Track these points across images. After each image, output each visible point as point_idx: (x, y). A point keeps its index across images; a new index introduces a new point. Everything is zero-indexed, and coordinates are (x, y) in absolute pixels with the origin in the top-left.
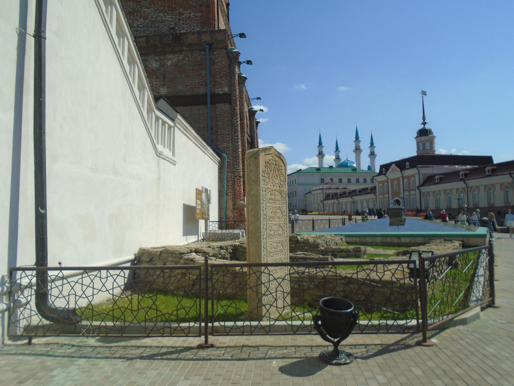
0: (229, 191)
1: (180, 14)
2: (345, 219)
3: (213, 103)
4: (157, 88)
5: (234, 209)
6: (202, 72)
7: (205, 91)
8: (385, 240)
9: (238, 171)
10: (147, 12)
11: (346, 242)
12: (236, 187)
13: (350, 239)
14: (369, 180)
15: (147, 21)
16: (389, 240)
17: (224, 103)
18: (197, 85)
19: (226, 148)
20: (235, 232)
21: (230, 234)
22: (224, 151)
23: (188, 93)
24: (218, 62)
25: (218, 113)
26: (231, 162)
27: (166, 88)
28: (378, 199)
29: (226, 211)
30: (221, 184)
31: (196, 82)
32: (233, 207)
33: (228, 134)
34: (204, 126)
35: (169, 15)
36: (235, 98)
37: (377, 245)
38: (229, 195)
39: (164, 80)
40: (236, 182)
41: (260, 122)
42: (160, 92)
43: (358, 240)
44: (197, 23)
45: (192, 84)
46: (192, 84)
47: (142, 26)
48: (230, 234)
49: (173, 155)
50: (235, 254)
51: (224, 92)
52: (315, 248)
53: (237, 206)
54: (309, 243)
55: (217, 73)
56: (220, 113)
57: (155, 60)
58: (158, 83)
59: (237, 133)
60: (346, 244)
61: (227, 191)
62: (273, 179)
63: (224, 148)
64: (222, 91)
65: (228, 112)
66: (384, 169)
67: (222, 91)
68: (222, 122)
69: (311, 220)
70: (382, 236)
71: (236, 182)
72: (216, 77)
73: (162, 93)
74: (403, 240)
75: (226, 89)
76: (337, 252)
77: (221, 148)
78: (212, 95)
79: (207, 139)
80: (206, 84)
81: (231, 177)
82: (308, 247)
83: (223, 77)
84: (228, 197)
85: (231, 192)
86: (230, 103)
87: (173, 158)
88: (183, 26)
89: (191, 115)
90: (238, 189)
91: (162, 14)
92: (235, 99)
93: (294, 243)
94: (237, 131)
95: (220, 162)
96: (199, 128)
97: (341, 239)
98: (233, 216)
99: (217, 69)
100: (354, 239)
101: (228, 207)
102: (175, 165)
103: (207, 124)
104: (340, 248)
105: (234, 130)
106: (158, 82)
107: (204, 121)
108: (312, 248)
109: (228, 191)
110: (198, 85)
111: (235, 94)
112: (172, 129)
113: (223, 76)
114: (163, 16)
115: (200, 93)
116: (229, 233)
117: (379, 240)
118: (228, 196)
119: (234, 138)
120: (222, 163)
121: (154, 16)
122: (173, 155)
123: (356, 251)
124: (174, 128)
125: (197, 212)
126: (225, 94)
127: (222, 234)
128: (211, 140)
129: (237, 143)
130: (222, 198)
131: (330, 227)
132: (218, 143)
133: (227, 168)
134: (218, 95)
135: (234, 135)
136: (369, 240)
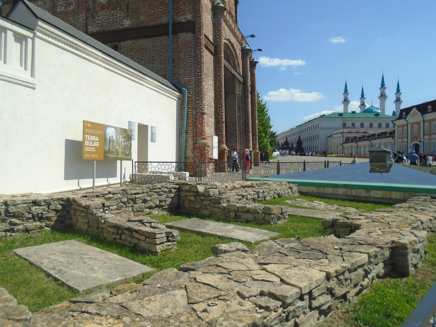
0: (190, 129)
2: (328, 162)
3: (175, 33)
4: (121, 20)
5: (194, 148)
7: (168, 20)
8: (349, 192)
9: (200, 107)
11: (298, 192)
12: (197, 124)
13: (305, 189)
16: (354, 192)
18: (159, 14)
19: (188, 81)
20: (163, 175)
21: (157, 177)
23: (150, 24)
25: (180, 43)
27: (130, 19)
28: (396, 143)
29: (186, 150)
30: (181, 122)
31: (159, 11)
32: (194, 147)
33: (189, 67)
36: (199, 25)
37: (337, 199)
38: (190, 133)
39: (128, 12)
40: (198, 119)
41: (258, 63)
42: (124, 24)
45: (155, 13)
46: (155, 13)
48: (157, 177)
49: (32, 75)
50: (68, 212)
51: (187, 20)
53: (197, 145)
54: (211, 196)
56: (182, 43)
58: (122, 15)
59: (200, 65)
60: (299, 194)
61: (187, 129)
63: (185, 82)
64: (184, 19)
65: (190, 42)
66: (404, 113)
67: (184, 19)
68: (184, 53)
69: (302, 162)
70: (345, 186)
71: (198, 119)
72: (180, 3)
73: (125, 26)
74: (373, 194)
76: (241, 212)
78: (174, 24)
79: (169, 73)
81: (193, 114)
82: (209, 202)
83: (187, 3)
84: (188, 136)
85: (191, 130)
86: (194, 32)
87: (31, 80)
92: (199, 27)
94: (200, 62)
95: (181, 98)
96: (161, 61)
97: (291, 188)
98: (192, 156)
100: (311, 189)
101: (188, 146)
102: (34, 89)
103: (169, 56)
105: (198, 62)
106: (121, 14)
107: (167, 53)
108: (213, 203)
109: (189, 128)
110: (161, 14)
111: (199, 21)
112: (30, 41)
115: (163, 23)
116: (156, 176)
117: (341, 191)
118: (189, 134)
119: (197, 71)
122: (32, 75)
123: (265, 213)
124: (33, 39)
125: (86, 150)
126: (188, 22)
127: (149, 177)
128: (172, 74)
130: (182, 137)
131: (304, 170)
132: (180, 77)
133: (188, 104)
134: (181, 23)
136: (329, 190)
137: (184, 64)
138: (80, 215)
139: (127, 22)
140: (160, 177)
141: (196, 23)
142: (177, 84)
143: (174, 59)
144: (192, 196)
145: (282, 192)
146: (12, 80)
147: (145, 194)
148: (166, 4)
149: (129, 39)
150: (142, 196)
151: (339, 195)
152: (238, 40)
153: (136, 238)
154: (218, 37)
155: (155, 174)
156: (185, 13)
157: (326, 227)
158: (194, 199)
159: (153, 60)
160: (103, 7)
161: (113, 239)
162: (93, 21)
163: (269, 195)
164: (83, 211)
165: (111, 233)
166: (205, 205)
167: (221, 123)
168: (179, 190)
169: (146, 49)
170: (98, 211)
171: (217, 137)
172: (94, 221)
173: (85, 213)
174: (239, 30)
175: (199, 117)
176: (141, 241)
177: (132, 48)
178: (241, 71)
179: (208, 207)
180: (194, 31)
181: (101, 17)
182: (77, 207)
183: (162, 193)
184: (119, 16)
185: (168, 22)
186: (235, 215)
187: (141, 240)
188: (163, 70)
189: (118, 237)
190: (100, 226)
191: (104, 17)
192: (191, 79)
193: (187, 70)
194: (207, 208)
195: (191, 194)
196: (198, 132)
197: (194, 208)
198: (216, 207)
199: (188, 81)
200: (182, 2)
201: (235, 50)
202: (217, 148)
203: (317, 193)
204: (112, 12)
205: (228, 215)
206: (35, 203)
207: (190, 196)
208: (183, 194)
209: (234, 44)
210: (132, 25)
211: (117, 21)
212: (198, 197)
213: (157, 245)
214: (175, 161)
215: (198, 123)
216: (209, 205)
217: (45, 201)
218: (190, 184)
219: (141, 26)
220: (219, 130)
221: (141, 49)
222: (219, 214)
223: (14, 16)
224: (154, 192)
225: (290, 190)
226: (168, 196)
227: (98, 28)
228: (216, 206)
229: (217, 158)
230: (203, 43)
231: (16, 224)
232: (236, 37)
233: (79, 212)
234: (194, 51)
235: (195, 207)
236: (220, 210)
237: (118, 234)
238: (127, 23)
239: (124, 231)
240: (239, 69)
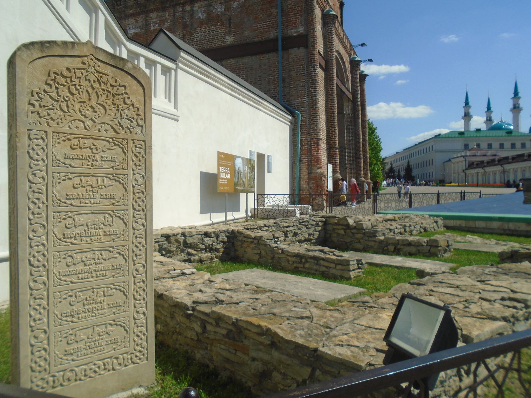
0: (304, 157)
2: (464, 193)
4: (223, 37)
5: (309, 179)
6: (272, 10)
8: (506, 226)
9: (315, 131)
11: (445, 226)
12: (312, 151)
13: (451, 223)
16: (512, 226)
17: (298, 47)
18: (266, 28)
19: (301, 103)
20: (288, 208)
21: (282, 211)
22: (298, 108)
23: (256, 40)
25: (291, 60)
26: (307, 121)
27: (232, 35)
29: (300, 181)
30: (294, 149)
32: (309, 177)
33: (303, 86)
34: (275, 78)
36: (312, 39)
37: (492, 233)
38: (304, 161)
39: (230, 27)
40: (312, 145)
41: (368, 75)
43: (463, 223)
45: (262, 27)
46: (262, 27)
50: (233, 243)
52: (371, 237)
53: (313, 175)
54: (364, 230)
55: (291, 10)
57: (220, 3)
59: (314, 84)
60: (445, 229)
61: (301, 157)
62: (89, 113)
63: (298, 104)
64: (295, 32)
65: (302, 58)
67: (295, 32)
68: (295, 71)
70: (501, 219)
71: (312, 145)
72: (290, 15)
73: (228, 43)
77: (294, 104)
78: (283, 39)
79: (278, 94)
80: (277, 25)
81: (307, 139)
82: (362, 235)
83: (298, 15)
84: (302, 165)
85: (306, 159)
86: (306, 47)
87: (174, 111)
89: (260, 66)
92: (312, 41)
93: (342, 229)
94: (314, 81)
95: (293, 122)
96: (269, 81)
97: (436, 222)
98: (308, 188)
99: (290, 4)
100: (458, 223)
101: (302, 176)
102: (177, 121)
103: (278, 75)
104: (407, 240)
105: (312, 80)
106: (223, 30)
107: (276, 72)
108: (368, 236)
109: (303, 156)
111: (312, 34)
113: (298, 13)
115: (271, 37)
116: (281, 209)
117: (495, 225)
118: (303, 163)
119: (311, 91)
120: (295, 123)
122: (175, 107)
123: (431, 246)
124: (176, 71)
125: (220, 182)
127: (274, 211)
128: (283, 95)
129: (314, 97)
130: (294, 166)
131: (438, 202)
132: (292, 98)
133: (301, 129)
134: (292, 38)
135: (311, 87)
136: (481, 224)
138: (249, 247)
139: (229, 38)
140: (286, 211)
142: (289, 107)
144: (341, 229)
145: (428, 226)
146: (163, 113)
147: (295, 227)
148: (274, 17)
149: (233, 58)
150: (292, 229)
151: (493, 229)
152: (346, 51)
153: (324, 266)
154: (329, 49)
155: (280, 208)
156: (297, 26)
157: (504, 258)
158: (344, 233)
159: (260, 80)
160: (201, 23)
161: (294, 267)
162: (190, 39)
163: (416, 229)
164: (252, 242)
165: (291, 263)
166: (357, 239)
167: (334, 149)
168: (325, 223)
169: (251, 68)
170: (271, 241)
171: (332, 165)
172: (267, 252)
173: (255, 244)
174: (347, 38)
175: (314, 143)
176: (331, 269)
177: (236, 67)
178: (350, 87)
179: (361, 241)
182: (245, 239)
183: (310, 226)
185: (277, 36)
186: (395, 249)
187: (330, 268)
189: (302, 266)
190: (276, 256)
191: (203, 33)
192: (305, 101)
193: (300, 91)
194: (360, 242)
195: (340, 227)
196: (313, 160)
197: (344, 241)
198: (371, 241)
199: (301, 103)
200: (292, 13)
201: (344, 63)
202: (332, 178)
203: (466, 227)
204: (212, 27)
205: (386, 248)
206: (207, 235)
207: (338, 229)
208: (330, 227)
209: (343, 56)
211: (217, 37)
212: (348, 231)
213: (350, 271)
214: (288, 193)
215: (313, 150)
216: (362, 238)
217: (214, 233)
218: (338, 217)
219: (245, 42)
222: (375, 247)
223: (154, 46)
224: (304, 225)
225: (435, 224)
226: (315, 229)
227: (197, 46)
228: (370, 239)
229: (332, 190)
230: (317, 59)
231: (192, 255)
232: (345, 48)
233: (246, 243)
234: (307, 68)
235: (346, 241)
236: (377, 243)
237: (300, 262)
238: (229, 40)
239: (309, 260)
240: (348, 85)
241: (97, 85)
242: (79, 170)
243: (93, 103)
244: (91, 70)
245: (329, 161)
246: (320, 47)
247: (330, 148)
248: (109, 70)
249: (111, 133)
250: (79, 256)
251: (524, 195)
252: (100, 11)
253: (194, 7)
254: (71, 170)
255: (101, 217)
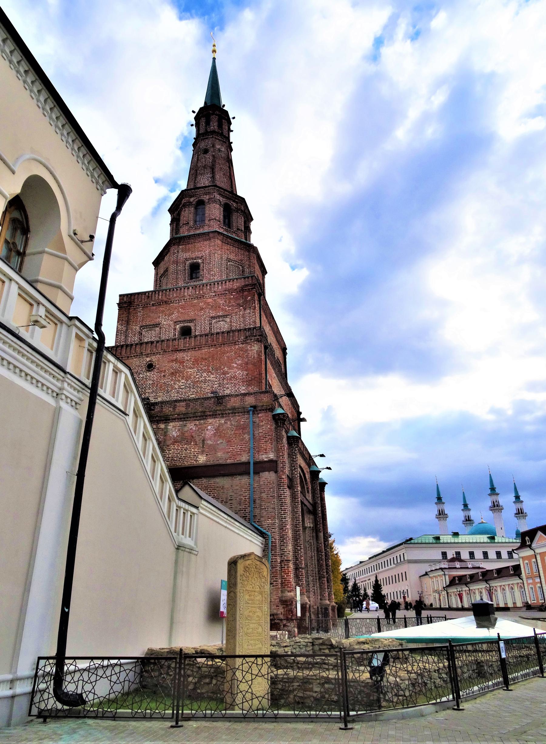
1: (224, 373)
2: (431, 617)
3: (256, 473)
6: (244, 436)
7: (248, 458)
9: (285, 553)
10: (190, 373)
14: (505, 555)
15: (189, 382)
17: (269, 471)
22: (268, 529)
23: (229, 461)
24: (263, 426)
25: (262, 483)
26: (277, 543)
28: (526, 585)
33: (273, 508)
34: (246, 499)
35: (213, 375)
39: (203, 447)
42: (199, 460)
44: (243, 382)
47: (183, 387)
56: (264, 483)
57: (195, 425)
63: (268, 525)
64: (266, 458)
66: (527, 538)
67: (266, 458)
73: (200, 462)
75: (271, 455)
77: (265, 525)
79: (249, 514)
80: (249, 450)
88: (227, 386)
90: (285, 577)
91: (205, 374)
92: (282, 466)
93: (328, 648)
94: (284, 504)
103: (249, 496)
105: (281, 503)
113: (268, 441)
114: (206, 375)
115: (243, 460)
121: (197, 377)
126: (271, 461)
128: (254, 516)
132: (262, 519)
133: (272, 550)
137: (267, 505)
141: (279, 462)
142: (259, 528)
143: (256, 500)
158: (328, 652)
159: (231, 500)
167: (300, 569)
175: (284, 565)
177: (208, 486)
180: (277, 470)
181: (172, 451)
183: (301, 647)
184: (193, 451)
185: (249, 460)
188: (242, 511)
192: (275, 522)
195: (325, 647)
196: (284, 583)
204: (186, 446)
207: (324, 649)
209: (304, 469)
210: (207, 461)
212: (332, 650)
219: (218, 462)
220: (297, 578)
221: (217, 487)
234: (276, 491)
238: (202, 459)
241: (255, 570)
242: (251, 605)
243: (254, 577)
244: (254, 564)
245: (298, 584)
246: (287, 471)
247: (297, 568)
248: (258, 563)
249: (258, 589)
250: (250, 642)
251: (476, 620)
252: (168, 484)
253: (168, 425)
254: (249, 605)
255: (256, 625)
